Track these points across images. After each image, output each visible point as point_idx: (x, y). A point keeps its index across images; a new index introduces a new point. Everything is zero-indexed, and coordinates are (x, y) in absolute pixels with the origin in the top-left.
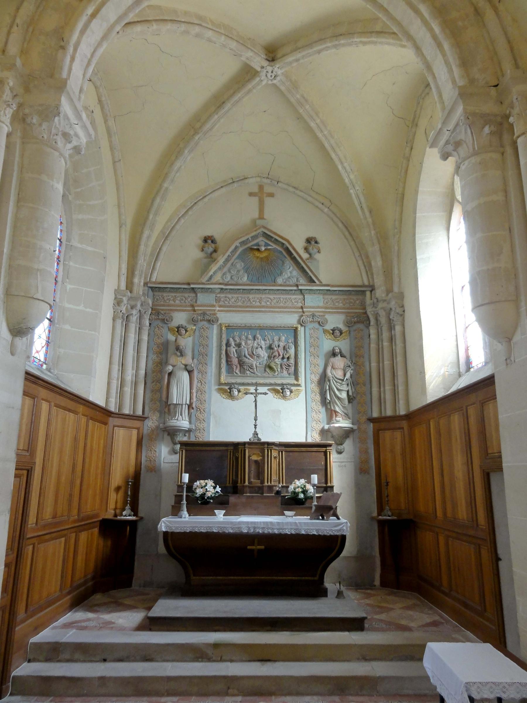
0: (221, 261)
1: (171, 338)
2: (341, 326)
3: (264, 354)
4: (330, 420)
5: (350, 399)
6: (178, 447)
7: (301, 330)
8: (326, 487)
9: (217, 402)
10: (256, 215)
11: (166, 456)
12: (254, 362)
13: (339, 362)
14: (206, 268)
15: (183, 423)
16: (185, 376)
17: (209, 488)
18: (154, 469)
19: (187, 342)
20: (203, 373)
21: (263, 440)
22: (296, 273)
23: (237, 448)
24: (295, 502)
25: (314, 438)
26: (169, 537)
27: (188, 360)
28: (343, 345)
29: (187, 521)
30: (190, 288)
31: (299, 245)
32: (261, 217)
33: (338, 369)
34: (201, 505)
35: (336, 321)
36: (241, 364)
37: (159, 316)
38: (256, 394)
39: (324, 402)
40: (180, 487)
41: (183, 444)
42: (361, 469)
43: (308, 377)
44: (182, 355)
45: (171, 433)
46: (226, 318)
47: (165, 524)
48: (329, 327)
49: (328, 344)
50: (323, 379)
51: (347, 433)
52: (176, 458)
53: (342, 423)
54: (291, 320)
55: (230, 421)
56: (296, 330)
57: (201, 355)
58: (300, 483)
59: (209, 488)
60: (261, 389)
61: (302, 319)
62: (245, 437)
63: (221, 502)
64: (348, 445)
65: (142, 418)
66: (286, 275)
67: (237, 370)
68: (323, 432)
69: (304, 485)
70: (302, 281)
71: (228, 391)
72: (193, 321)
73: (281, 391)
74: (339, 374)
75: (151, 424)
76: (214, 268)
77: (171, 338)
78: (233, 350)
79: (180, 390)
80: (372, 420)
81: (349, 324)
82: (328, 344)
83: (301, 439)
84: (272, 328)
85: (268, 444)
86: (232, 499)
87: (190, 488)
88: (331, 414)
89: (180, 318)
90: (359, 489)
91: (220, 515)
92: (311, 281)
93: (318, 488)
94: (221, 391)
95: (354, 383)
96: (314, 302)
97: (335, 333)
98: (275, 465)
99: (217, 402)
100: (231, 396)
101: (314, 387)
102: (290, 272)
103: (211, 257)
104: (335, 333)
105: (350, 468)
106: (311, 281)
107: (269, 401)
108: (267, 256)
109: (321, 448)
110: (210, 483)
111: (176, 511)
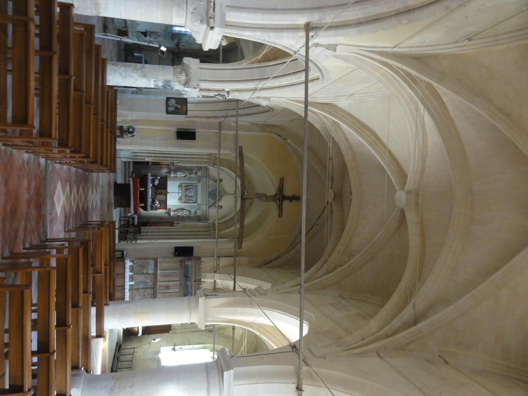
0: (215, 184)
1: (194, 172)
2: (197, 214)
3: (190, 195)
4: (173, 211)
5: (178, 216)
6: (166, 174)
7: (196, 204)
8: (157, 208)
9: (177, 183)
10: (228, 193)
11: (164, 171)
12: (188, 192)
13: (188, 213)
14: (212, 180)
15: (172, 175)
16: (184, 176)
17: (157, 183)
18: (161, 168)
19: (193, 175)
20: (185, 180)
21: (168, 195)
22: (212, 203)
23: (165, 188)
24: (153, 202)
25: (168, 207)
26: (147, 175)
27: (188, 176)
28: (192, 215)
29: (150, 178)
30: (208, 176)
31: (220, 204)
32: (227, 194)
33: (185, 213)
34: (153, 181)
35: (199, 213)
36: (187, 189)
37: (200, 169)
38: (179, 193)
39: (178, 209)
40: (157, 176)
41: (166, 176)
42: (161, 218)
43: (184, 205)
44: (189, 175)
45: (169, 172)
46: (200, 185)
47: (149, 174)
48: (197, 211)
49: (193, 211)
50: (183, 209)
51: (169, 215)
52: (164, 174)
53: (172, 214)
54: (199, 201)
55: (173, 187)
56: (196, 203)
57: (189, 179)
58: (158, 202)
59: (157, 183)
60: (180, 194)
61: (200, 204)
62: (169, 190)
63: (154, 185)
64: (167, 215)
65: (173, 165)
66: (212, 201)
67: (186, 188)
68: (170, 209)
69: (157, 204)
70: (210, 205)
71: (180, 186)
72: (199, 177)
73: (180, 199)
74: (185, 213)
75: (172, 167)
76: (213, 182)
77: (194, 172)
78: (191, 187)
79: (180, 174)
80: (173, 221)
81: (198, 217)
82: (193, 211)
83: (168, 203)
84: (197, 197)
85: (166, 196)
86: (154, 188)
87: (156, 179)
88: (174, 211)
89: (199, 173)
90: (156, 217)
91: (151, 185)
92: (209, 207)
93: (156, 206)
94: (180, 184)
95: (183, 217)
96: (204, 207)
97: (196, 213)
98: (162, 197)
99: (177, 183)
100: (179, 187)
101: (181, 207)
102: (212, 202)
103: (216, 181)
104: (196, 213)
105: (161, 215)
106: (209, 207)
107: (177, 196)
108: (215, 195)
109: (165, 208)
110: (157, 183)
111: (152, 176)
